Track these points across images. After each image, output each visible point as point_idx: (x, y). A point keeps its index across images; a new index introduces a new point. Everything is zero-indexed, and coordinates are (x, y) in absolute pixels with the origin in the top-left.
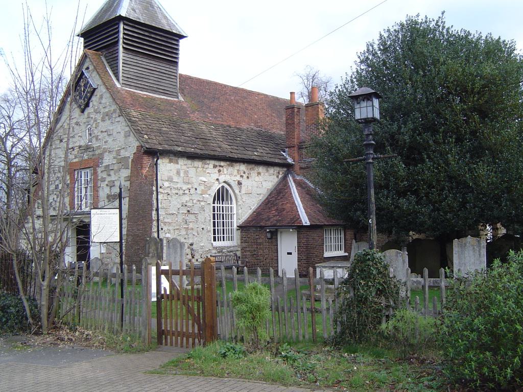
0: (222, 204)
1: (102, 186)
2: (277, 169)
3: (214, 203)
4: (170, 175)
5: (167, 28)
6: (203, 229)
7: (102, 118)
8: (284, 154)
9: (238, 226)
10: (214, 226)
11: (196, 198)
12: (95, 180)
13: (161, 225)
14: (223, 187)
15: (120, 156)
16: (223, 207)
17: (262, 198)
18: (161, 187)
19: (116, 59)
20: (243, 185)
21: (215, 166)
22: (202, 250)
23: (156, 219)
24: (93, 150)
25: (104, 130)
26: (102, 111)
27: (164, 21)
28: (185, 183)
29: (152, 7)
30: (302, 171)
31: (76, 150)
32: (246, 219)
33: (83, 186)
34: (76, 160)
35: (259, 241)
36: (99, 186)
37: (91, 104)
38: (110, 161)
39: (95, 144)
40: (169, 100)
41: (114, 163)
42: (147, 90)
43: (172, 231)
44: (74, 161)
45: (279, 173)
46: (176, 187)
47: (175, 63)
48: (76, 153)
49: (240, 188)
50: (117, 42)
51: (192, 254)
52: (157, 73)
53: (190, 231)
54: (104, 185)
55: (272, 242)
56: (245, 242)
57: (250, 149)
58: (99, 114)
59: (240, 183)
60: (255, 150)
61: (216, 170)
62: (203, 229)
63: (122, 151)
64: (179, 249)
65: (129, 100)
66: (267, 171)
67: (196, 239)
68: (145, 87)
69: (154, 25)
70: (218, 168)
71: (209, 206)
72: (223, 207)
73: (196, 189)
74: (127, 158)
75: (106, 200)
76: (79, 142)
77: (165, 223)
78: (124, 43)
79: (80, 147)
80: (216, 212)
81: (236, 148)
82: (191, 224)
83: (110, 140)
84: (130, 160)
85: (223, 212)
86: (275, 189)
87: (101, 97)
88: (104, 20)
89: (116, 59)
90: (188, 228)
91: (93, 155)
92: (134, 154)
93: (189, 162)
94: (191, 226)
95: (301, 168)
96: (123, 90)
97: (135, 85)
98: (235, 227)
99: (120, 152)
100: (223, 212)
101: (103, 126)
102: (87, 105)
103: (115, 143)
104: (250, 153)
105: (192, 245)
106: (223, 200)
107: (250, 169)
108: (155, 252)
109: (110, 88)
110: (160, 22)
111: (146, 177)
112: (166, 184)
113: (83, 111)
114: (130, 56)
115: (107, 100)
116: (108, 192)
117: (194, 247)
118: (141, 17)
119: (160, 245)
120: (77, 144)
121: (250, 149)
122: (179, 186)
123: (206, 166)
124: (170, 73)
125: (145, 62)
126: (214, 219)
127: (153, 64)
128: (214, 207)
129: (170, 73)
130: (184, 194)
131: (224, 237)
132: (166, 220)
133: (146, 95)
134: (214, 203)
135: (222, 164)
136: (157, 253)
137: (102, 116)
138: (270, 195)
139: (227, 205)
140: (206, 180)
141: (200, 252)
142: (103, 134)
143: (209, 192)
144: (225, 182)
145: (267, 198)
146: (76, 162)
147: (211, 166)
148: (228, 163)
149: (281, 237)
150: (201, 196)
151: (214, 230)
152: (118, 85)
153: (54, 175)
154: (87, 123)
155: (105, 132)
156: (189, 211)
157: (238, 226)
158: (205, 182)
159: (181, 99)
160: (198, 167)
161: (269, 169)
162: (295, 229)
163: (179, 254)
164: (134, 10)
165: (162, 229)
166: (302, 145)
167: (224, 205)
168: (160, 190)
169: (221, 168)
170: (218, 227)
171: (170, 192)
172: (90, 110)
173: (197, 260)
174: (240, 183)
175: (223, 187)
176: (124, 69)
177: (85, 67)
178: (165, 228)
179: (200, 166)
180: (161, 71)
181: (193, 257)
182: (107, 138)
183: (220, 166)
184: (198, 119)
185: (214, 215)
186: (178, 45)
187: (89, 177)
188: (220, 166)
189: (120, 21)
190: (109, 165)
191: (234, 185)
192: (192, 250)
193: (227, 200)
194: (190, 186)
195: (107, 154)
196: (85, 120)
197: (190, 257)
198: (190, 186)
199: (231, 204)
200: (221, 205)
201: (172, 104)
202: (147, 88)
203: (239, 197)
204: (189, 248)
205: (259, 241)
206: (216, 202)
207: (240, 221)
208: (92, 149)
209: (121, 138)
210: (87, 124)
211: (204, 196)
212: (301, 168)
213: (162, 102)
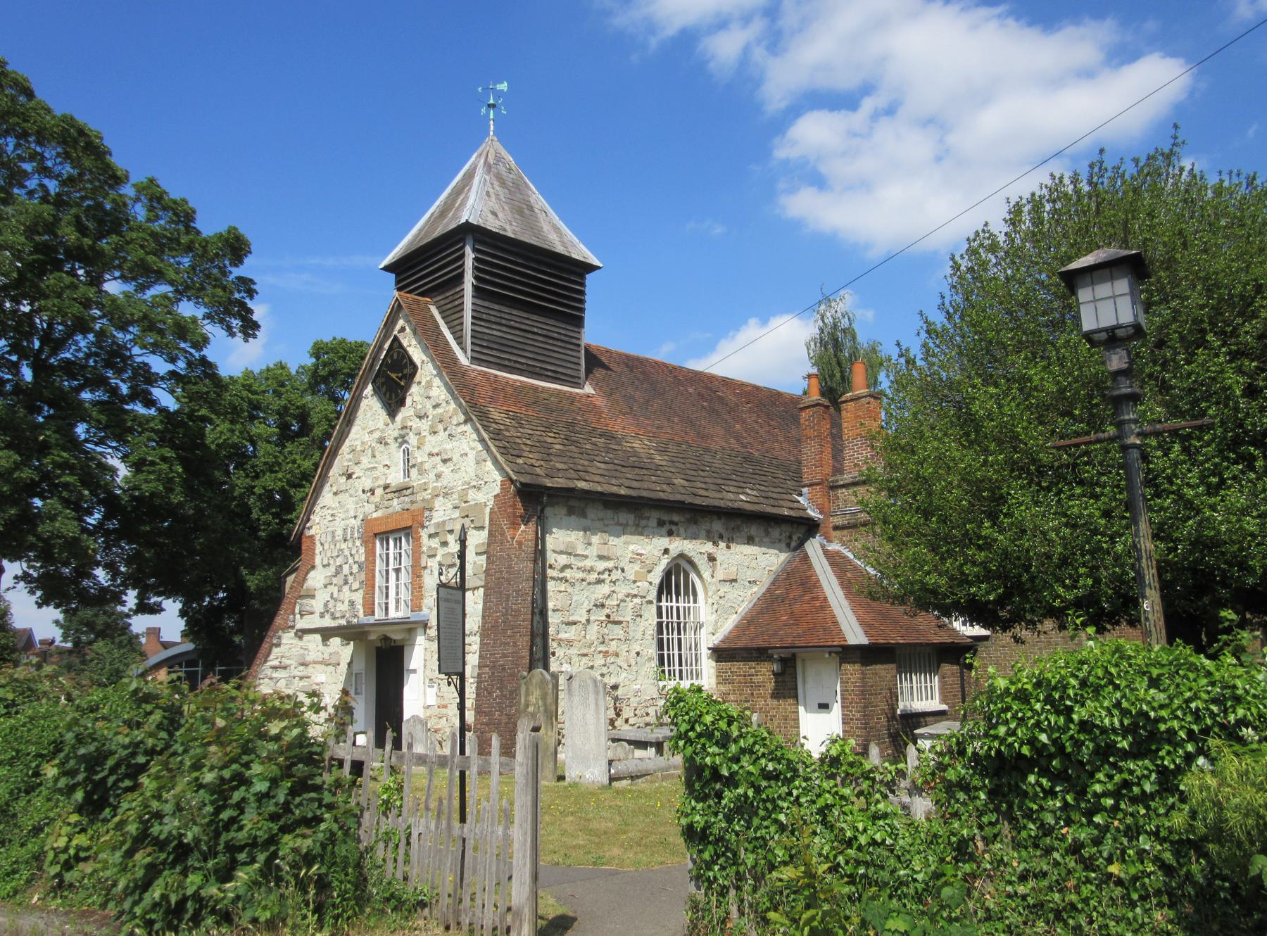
0: (677, 601)
1: (429, 564)
2: (786, 529)
3: (659, 600)
4: (569, 539)
5: (560, 249)
6: (638, 654)
7: (431, 427)
8: (799, 498)
9: (709, 649)
10: (661, 647)
11: (622, 590)
12: (416, 555)
13: (553, 645)
14: (678, 566)
15: (466, 502)
16: (678, 608)
17: (758, 590)
18: (551, 566)
19: (459, 308)
20: (718, 562)
21: (661, 523)
22: (638, 699)
23: (541, 631)
24: (413, 494)
25: (435, 451)
26: (431, 412)
27: (553, 237)
28: (601, 557)
29: (531, 208)
30: (838, 533)
31: (379, 492)
32: (726, 633)
33: (391, 567)
35: (755, 679)
36: (423, 565)
37: (409, 401)
38: (447, 512)
39: (415, 479)
40: (565, 393)
41: (453, 516)
42: (520, 372)
43: (575, 659)
44: (375, 515)
45: (790, 537)
46: (581, 564)
47: (578, 321)
48: (378, 500)
49: (714, 567)
50: (460, 277)
51: (615, 709)
52: (541, 339)
53: (611, 659)
55: (783, 682)
56: (726, 681)
57: (731, 489)
58: (424, 421)
59: (712, 559)
60: (740, 490)
61: (664, 530)
62: (638, 654)
63: (471, 492)
64: (592, 697)
65: (485, 391)
66: (767, 534)
67: (624, 675)
68: (517, 366)
69: (533, 242)
70: (667, 527)
71: (650, 606)
72: (678, 608)
73: (623, 570)
74: (479, 507)
76: (384, 477)
77: (560, 642)
78: (476, 278)
79: (386, 487)
80: (664, 619)
81: (703, 486)
82: (614, 642)
83: (445, 470)
84: (487, 511)
85: (678, 617)
86: (784, 570)
87: (429, 385)
88: (436, 234)
89: (459, 308)
90: (607, 652)
91: (412, 502)
92: (496, 496)
93: (609, 513)
94: (613, 646)
95: (836, 528)
96: (473, 371)
97: (498, 361)
98: (705, 653)
99: (467, 495)
100: (678, 617)
101: (432, 443)
102: (402, 402)
103: (457, 476)
104: (731, 496)
105: (615, 687)
106: (678, 594)
107: (733, 529)
108: (540, 703)
109: (446, 363)
110: (545, 239)
111: (520, 543)
112: (563, 560)
113: (392, 414)
114: (486, 304)
115: (439, 391)
117: (620, 692)
118: (508, 227)
119: (550, 686)
120: (381, 482)
121: (731, 489)
122: (588, 563)
123: (643, 522)
124: (566, 339)
125: (517, 316)
126: (660, 631)
127: (536, 322)
128: (659, 609)
129: (566, 339)
130: (600, 582)
131: (681, 671)
132: (562, 636)
133: (521, 382)
134: (659, 600)
135: (676, 518)
136: (545, 705)
137: (430, 423)
138: (773, 583)
139: (687, 605)
140: (643, 552)
141: (634, 701)
142: (433, 458)
143: (651, 577)
144: (682, 556)
145: (769, 590)
146: (376, 519)
147: (653, 523)
148: (688, 516)
149: (804, 673)
150: (632, 585)
151: (661, 658)
152: (464, 360)
153: (333, 547)
154: (402, 440)
156: (608, 616)
157: (709, 649)
158: (641, 555)
159: (588, 389)
160: (627, 525)
161: (770, 530)
162: (835, 653)
163: (592, 706)
164: (494, 214)
165: (554, 654)
166: (837, 481)
167: (681, 605)
168: (550, 572)
169: (674, 528)
170: (669, 650)
171: (568, 576)
172: (404, 413)
173: (627, 721)
174: (712, 559)
175: (678, 566)
176: (477, 328)
177: (398, 327)
178: (560, 652)
179: (631, 522)
180: (550, 334)
181: (618, 715)
182: (441, 468)
183: (672, 523)
184: (624, 428)
185: (660, 625)
186: (583, 285)
187: (403, 548)
188: (672, 523)
189: (463, 240)
190: (444, 522)
191: (702, 563)
192: (616, 699)
193: (686, 593)
194: (610, 564)
195: (441, 498)
196: (396, 434)
197: (612, 714)
198: (610, 564)
199: (695, 601)
200: (674, 604)
201: (573, 398)
202: (521, 367)
203: (712, 589)
204: (609, 693)
205: (755, 679)
206: (664, 598)
207: (714, 638)
208: (409, 491)
209: (468, 469)
210: (400, 440)
211: (638, 584)
212: (836, 528)
213: (551, 395)
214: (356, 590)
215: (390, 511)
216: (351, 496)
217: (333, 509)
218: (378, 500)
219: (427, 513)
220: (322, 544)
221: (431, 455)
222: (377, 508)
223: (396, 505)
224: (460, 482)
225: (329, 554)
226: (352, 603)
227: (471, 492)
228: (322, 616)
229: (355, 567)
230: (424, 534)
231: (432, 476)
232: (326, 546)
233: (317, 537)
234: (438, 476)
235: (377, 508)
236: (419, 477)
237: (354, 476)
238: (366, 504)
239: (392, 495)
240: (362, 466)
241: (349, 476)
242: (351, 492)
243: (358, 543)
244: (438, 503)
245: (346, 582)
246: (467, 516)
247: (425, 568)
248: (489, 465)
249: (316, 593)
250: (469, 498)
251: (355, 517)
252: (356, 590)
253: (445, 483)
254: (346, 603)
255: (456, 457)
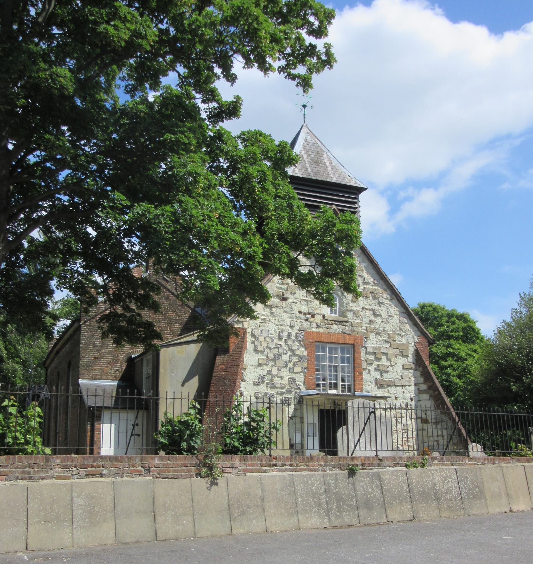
1: (368, 368)
25: (368, 307)
34: (320, 330)
44: (315, 330)
54: (372, 368)
74: (407, 346)
75: (373, 385)
83: (378, 320)
116: (379, 377)
155: (370, 310)
182: (373, 319)
195: (373, 334)
208: (346, 324)
214: (297, 373)
215: (332, 331)
216: (285, 312)
217: (263, 315)
218: (319, 322)
219: (366, 340)
220: (253, 335)
221: (363, 308)
222: (318, 326)
223: (335, 328)
224: (389, 330)
225: (265, 344)
226: (292, 381)
227: (396, 337)
228: (256, 384)
229: (295, 359)
230: (363, 351)
231: (367, 320)
232: (261, 339)
233: (249, 330)
234: (371, 322)
235: (318, 326)
236: (355, 318)
237: (289, 300)
238: (304, 321)
239: (333, 322)
240: (295, 296)
241: (284, 299)
242: (285, 309)
243: (297, 344)
244: (372, 336)
245: (286, 366)
246: (397, 348)
247: (365, 369)
248: (408, 327)
249: (247, 367)
250: (396, 339)
251: (292, 327)
252: (297, 373)
253: (377, 327)
254: (286, 379)
255: (384, 315)
